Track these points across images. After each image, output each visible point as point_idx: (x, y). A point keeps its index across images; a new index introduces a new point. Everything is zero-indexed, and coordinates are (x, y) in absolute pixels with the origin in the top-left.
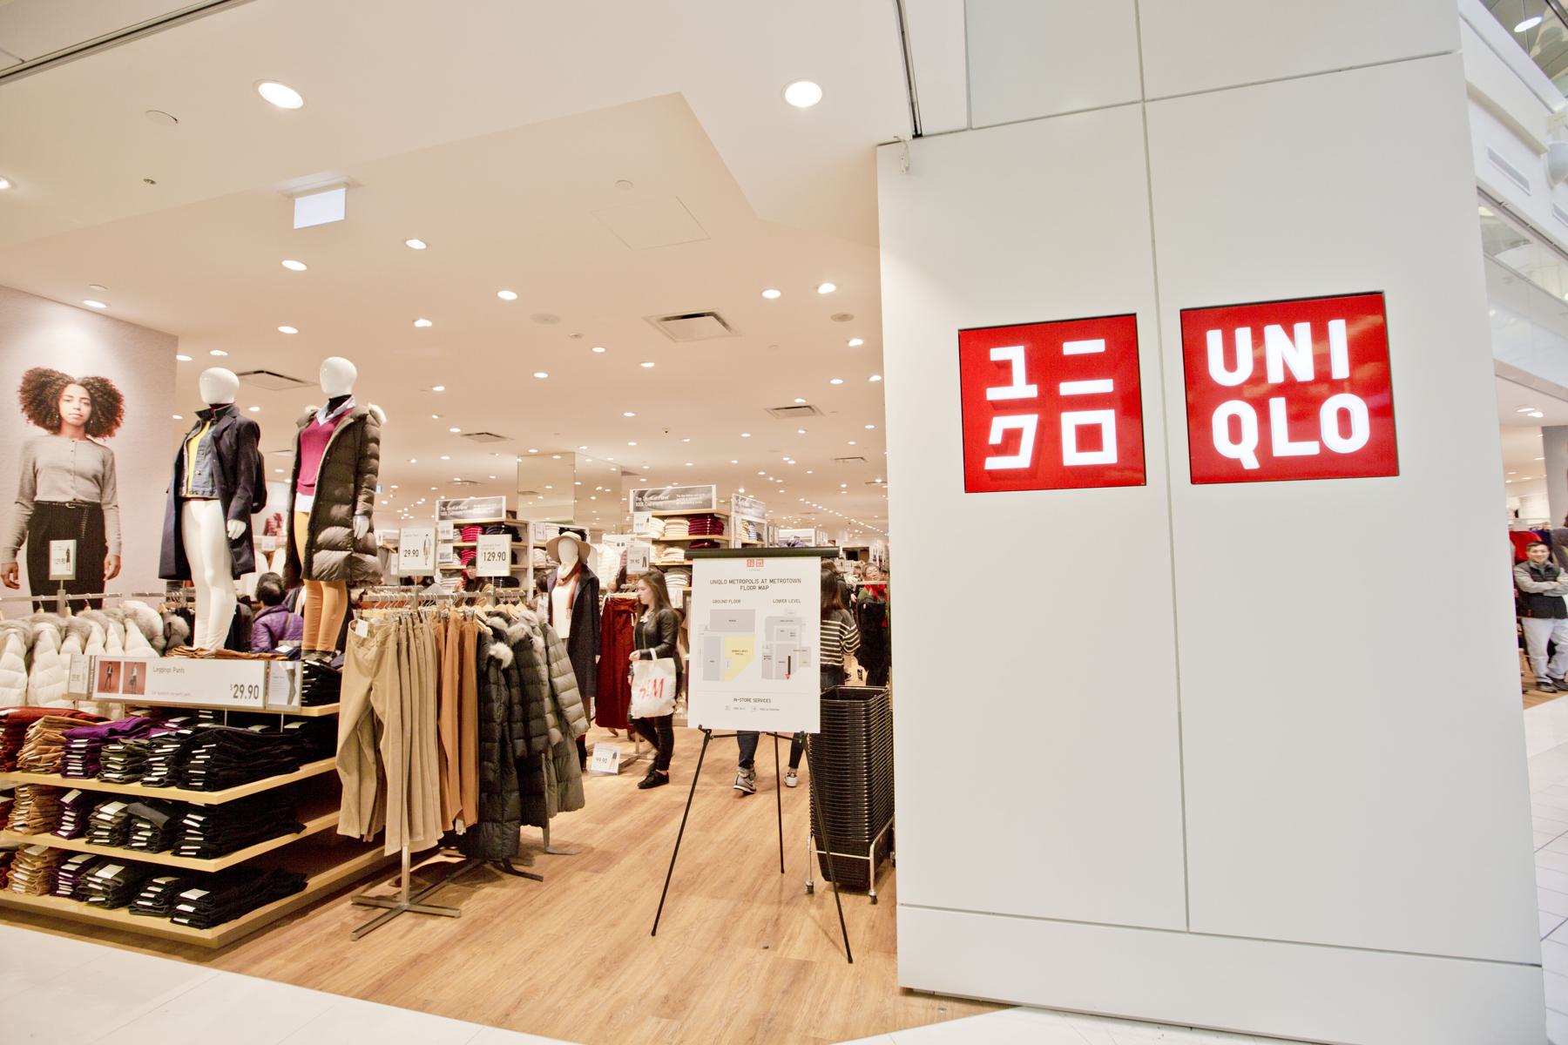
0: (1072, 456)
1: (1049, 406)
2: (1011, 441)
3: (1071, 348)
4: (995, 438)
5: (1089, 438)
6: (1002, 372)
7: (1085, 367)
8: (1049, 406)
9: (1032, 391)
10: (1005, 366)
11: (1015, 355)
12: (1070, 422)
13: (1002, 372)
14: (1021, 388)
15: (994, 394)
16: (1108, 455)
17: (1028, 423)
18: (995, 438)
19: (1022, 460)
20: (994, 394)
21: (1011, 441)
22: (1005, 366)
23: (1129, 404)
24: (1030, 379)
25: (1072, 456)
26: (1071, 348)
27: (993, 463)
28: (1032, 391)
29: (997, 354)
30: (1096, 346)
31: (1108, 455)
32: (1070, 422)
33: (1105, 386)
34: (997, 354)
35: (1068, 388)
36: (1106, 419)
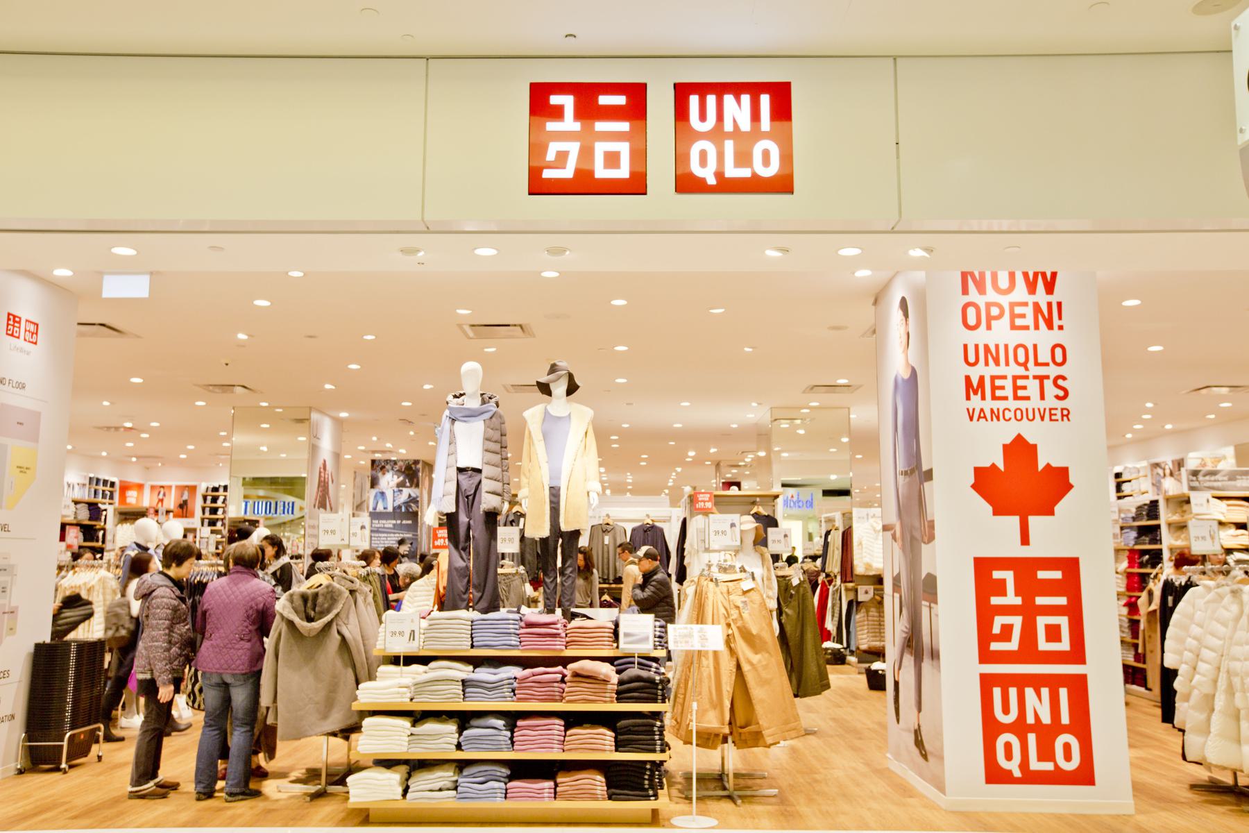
0: (1043, 645)
1: (1029, 612)
2: (1007, 632)
3: (1042, 575)
4: (996, 629)
5: (1053, 633)
6: (1000, 588)
7: (1050, 588)
8: (1029, 612)
9: (1018, 601)
10: (1003, 582)
11: (1008, 576)
12: (1042, 621)
13: (1000, 588)
14: (1012, 599)
15: (995, 601)
16: (1064, 645)
17: (1017, 621)
18: (996, 629)
19: (1013, 645)
20: (995, 601)
21: (1007, 632)
22: (1003, 582)
23: (1074, 612)
24: (1017, 594)
25: (1043, 645)
26: (1042, 575)
27: (995, 646)
28: (1018, 601)
29: (997, 575)
30: (1057, 575)
31: (1064, 645)
32: (1042, 621)
33: (1062, 601)
34: (997, 575)
35: (1040, 601)
36: (1063, 621)
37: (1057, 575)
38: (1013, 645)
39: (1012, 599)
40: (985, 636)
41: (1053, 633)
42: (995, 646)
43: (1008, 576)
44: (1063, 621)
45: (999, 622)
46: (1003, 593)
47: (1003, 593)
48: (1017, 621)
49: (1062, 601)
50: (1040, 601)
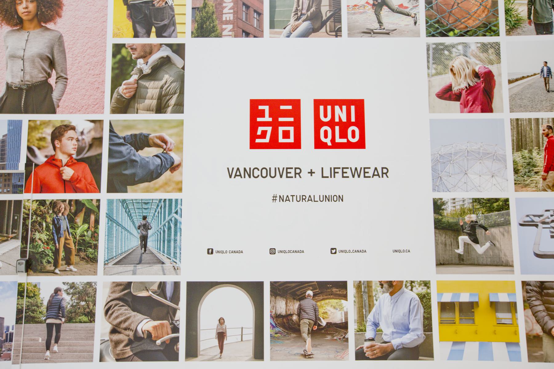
0: (281, 140)
1: (275, 125)
2: (264, 133)
3: (282, 107)
4: (259, 133)
5: (286, 135)
7: (286, 114)
8: (275, 125)
9: (270, 120)
10: (263, 111)
11: (266, 108)
12: (281, 129)
14: (267, 118)
15: (259, 119)
16: (291, 140)
17: (269, 129)
18: (259, 133)
19: (267, 140)
20: (259, 119)
21: (264, 133)
22: (263, 111)
23: (297, 125)
24: (270, 117)
25: (281, 140)
26: (282, 107)
27: (258, 141)
28: (270, 120)
29: (261, 107)
30: (290, 107)
31: (291, 140)
32: (281, 129)
33: (292, 119)
34: (261, 107)
35: (281, 119)
36: (291, 129)
37: (290, 107)
38: (267, 140)
39: (267, 118)
40: (253, 135)
41: (286, 135)
42: (258, 141)
43: (266, 108)
44: (291, 129)
45: (260, 129)
46: (263, 116)
47: (263, 116)
48: (269, 129)
49: (292, 119)
50: (281, 119)
